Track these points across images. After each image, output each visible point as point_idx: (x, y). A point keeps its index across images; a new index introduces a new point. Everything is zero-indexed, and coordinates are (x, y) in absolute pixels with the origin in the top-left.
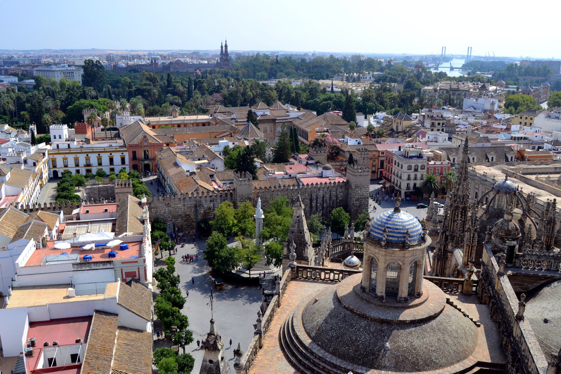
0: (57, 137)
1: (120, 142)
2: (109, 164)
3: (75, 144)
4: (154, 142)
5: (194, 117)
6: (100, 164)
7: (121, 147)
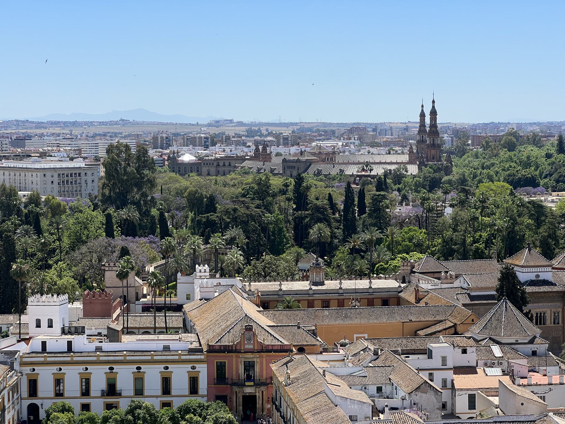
0: (44, 324)
1: (188, 340)
2: (159, 392)
3: (80, 342)
4: (269, 342)
5: (362, 284)
6: (139, 392)
7: (192, 351)
